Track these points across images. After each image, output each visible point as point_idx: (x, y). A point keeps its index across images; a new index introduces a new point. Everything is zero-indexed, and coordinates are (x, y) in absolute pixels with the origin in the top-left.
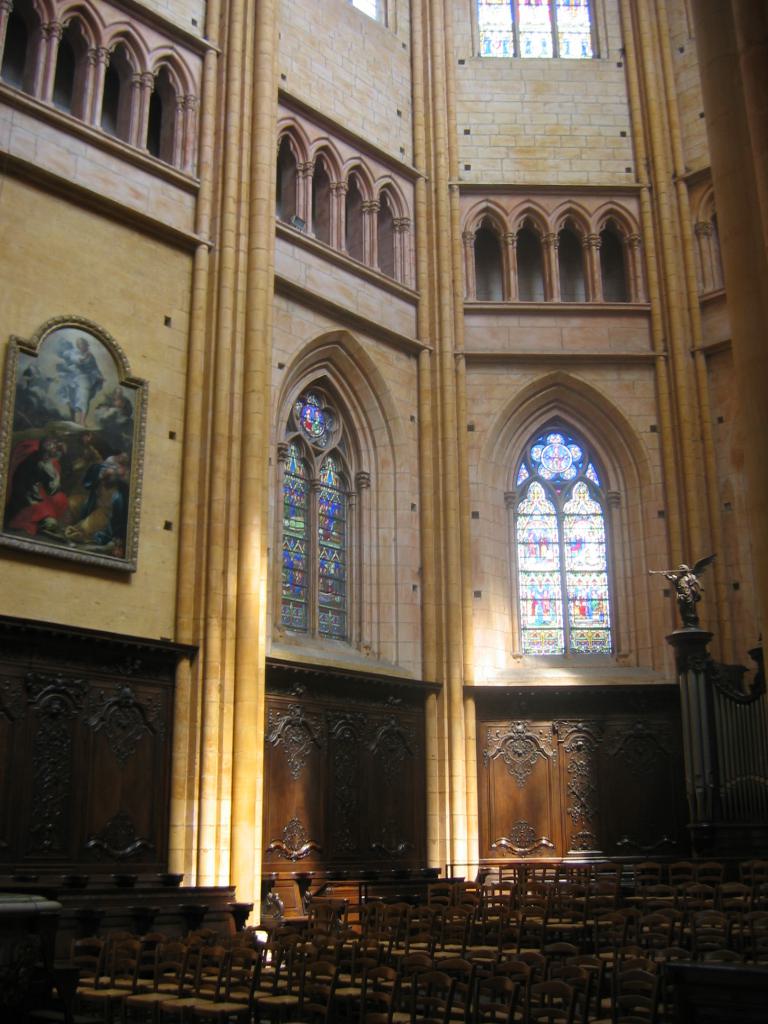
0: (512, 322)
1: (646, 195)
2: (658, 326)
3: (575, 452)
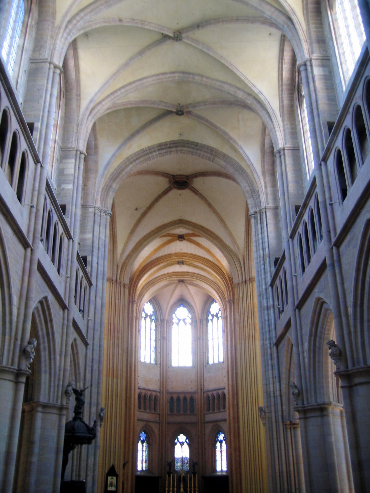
0: (142, 413)
1: (161, 393)
2: (161, 417)
3: (145, 435)
